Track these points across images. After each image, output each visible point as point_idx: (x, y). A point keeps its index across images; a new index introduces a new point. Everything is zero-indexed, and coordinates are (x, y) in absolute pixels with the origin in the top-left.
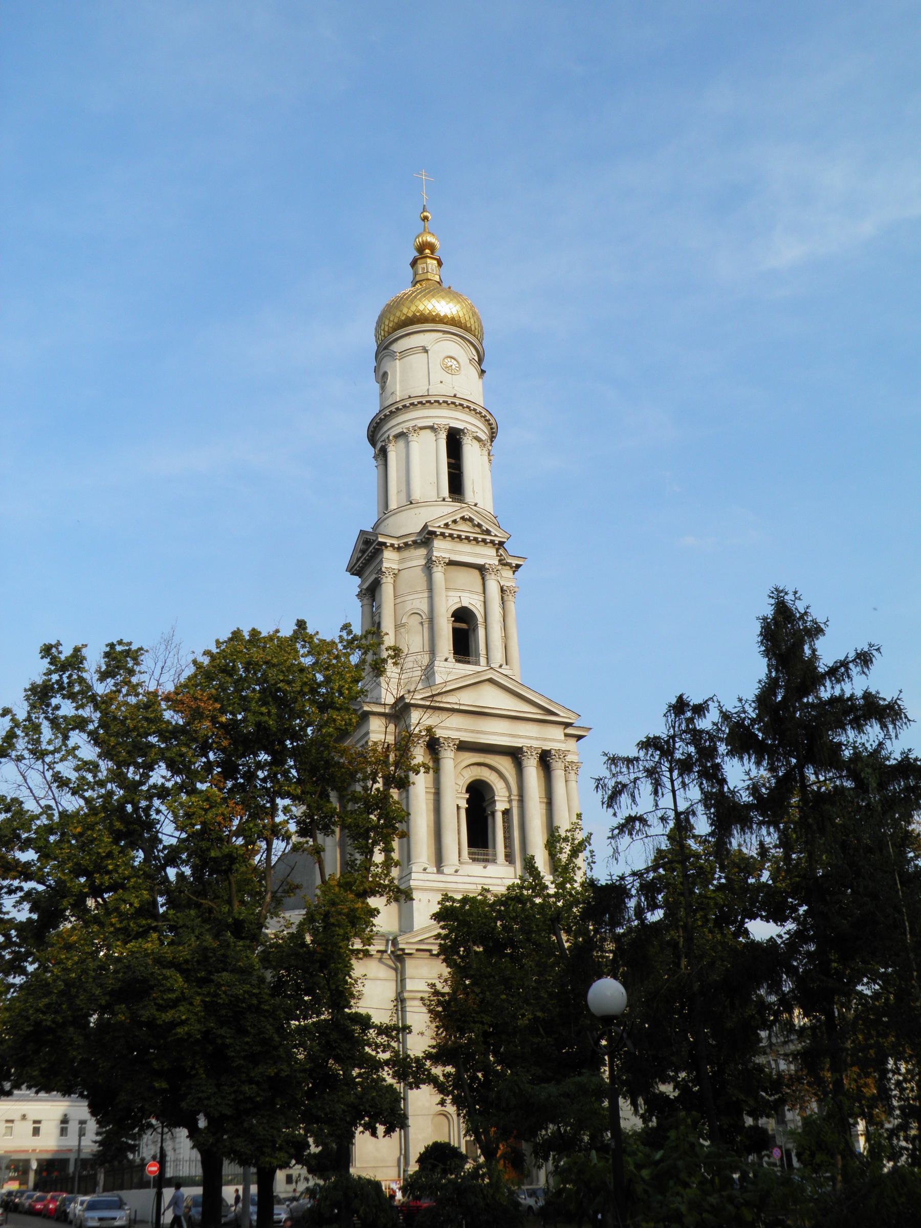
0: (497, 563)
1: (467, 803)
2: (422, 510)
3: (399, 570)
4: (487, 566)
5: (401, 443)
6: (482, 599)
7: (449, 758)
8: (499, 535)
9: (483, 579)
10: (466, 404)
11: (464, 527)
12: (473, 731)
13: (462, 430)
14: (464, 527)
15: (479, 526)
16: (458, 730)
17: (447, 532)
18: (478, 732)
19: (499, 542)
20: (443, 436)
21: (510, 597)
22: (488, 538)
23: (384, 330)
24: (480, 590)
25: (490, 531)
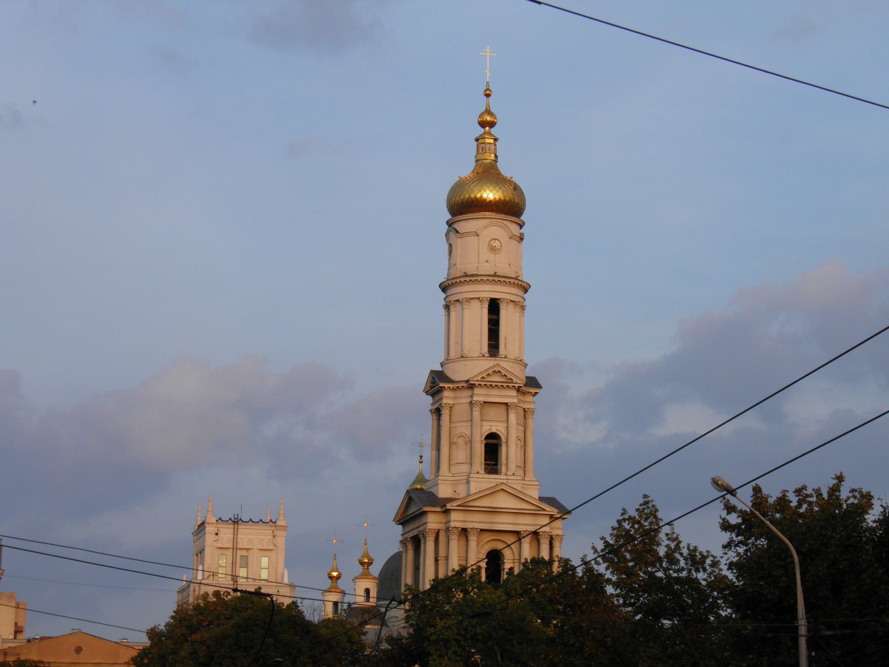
1: (487, 565)
2: (469, 363)
3: (453, 404)
5: (458, 305)
6: (506, 425)
7: (473, 540)
8: (518, 382)
11: (496, 378)
12: (489, 523)
13: (500, 299)
14: (496, 378)
16: (480, 522)
17: (483, 383)
18: (493, 523)
19: (518, 387)
20: (486, 305)
21: (530, 416)
22: (511, 385)
23: (455, 198)
24: (504, 419)
25: (512, 380)
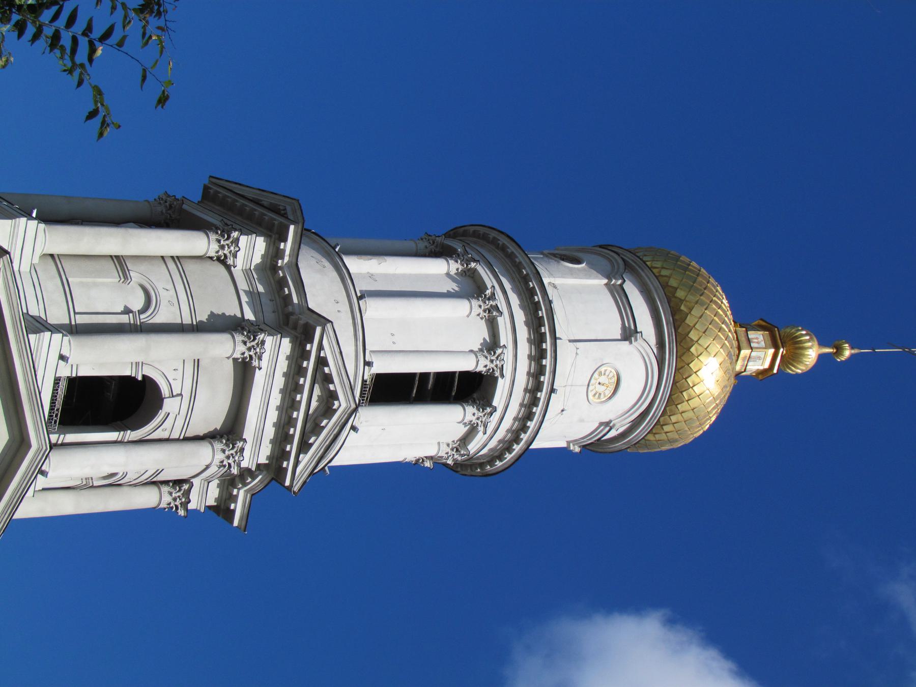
0: (244, 464)
4: (240, 444)
6: (175, 435)
9: (211, 436)
10: (538, 410)
15: (317, 429)
17: (310, 365)
22: (293, 448)
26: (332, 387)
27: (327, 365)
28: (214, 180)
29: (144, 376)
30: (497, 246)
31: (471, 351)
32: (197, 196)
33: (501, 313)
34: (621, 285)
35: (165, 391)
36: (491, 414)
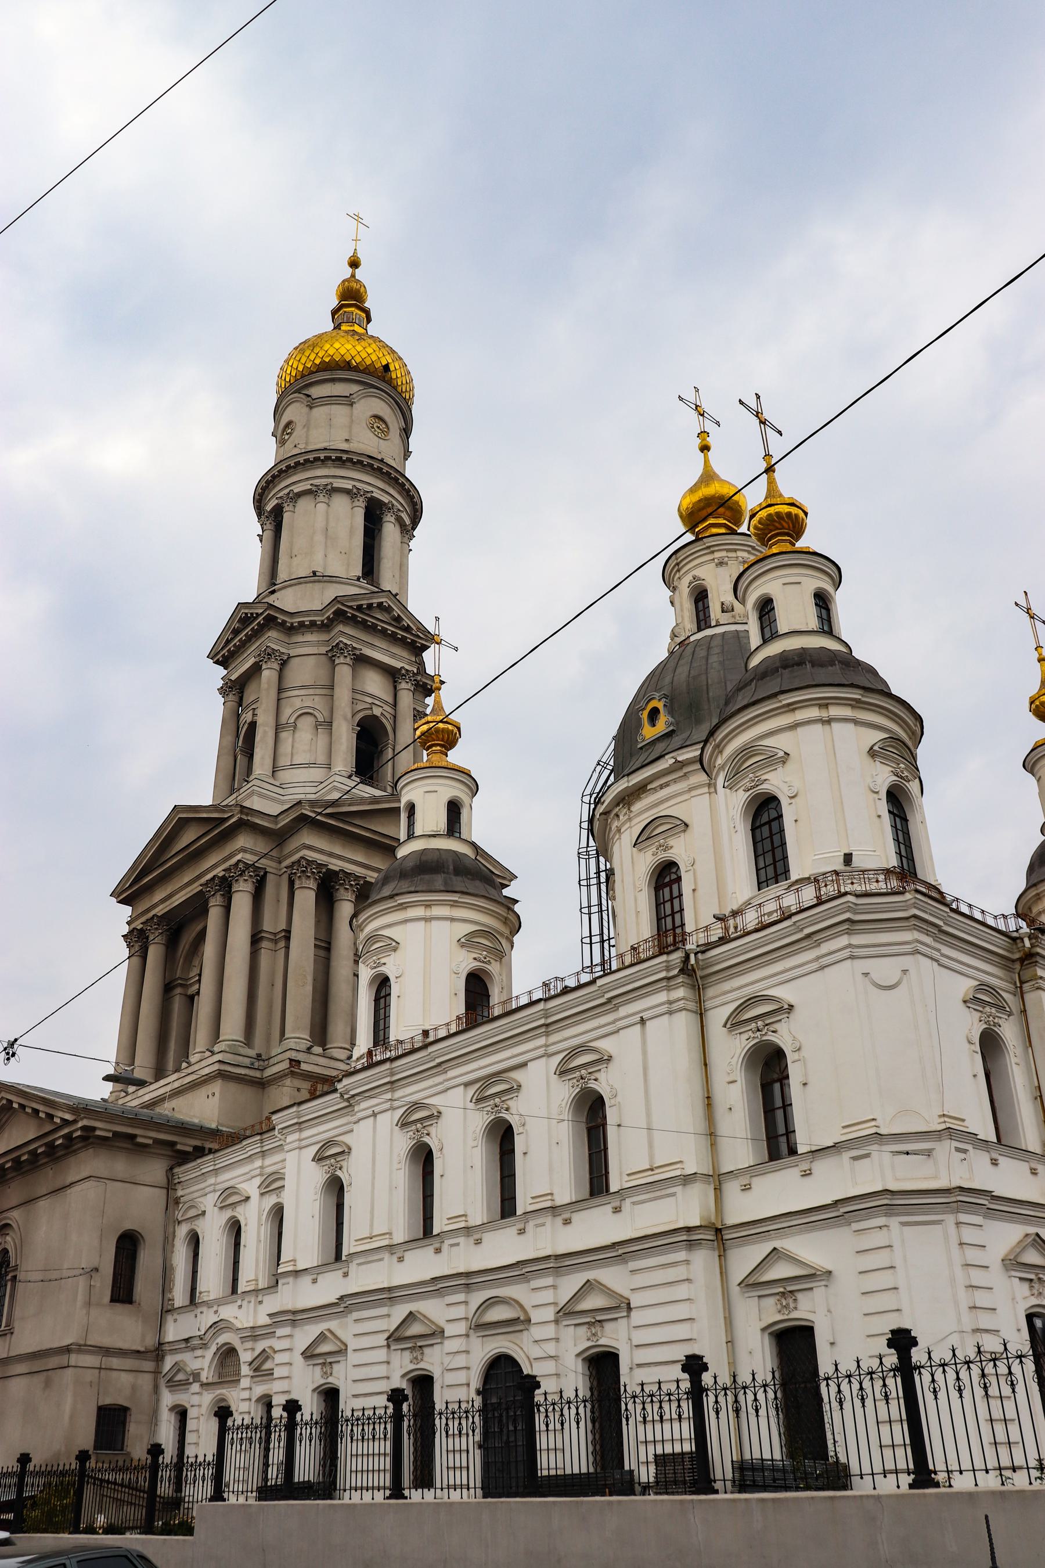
10: (394, 474)
13: (385, 504)
15: (398, 619)
24: (390, 700)
26: (375, 605)
27: (362, 605)
28: (210, 656)
29: (358, 726)
30: (278, 476)
31: (352, 509)
32: (221, 671)
33: (331, 483)
34: (314, 400)
35: (369, 713)
36: (393, 505)
